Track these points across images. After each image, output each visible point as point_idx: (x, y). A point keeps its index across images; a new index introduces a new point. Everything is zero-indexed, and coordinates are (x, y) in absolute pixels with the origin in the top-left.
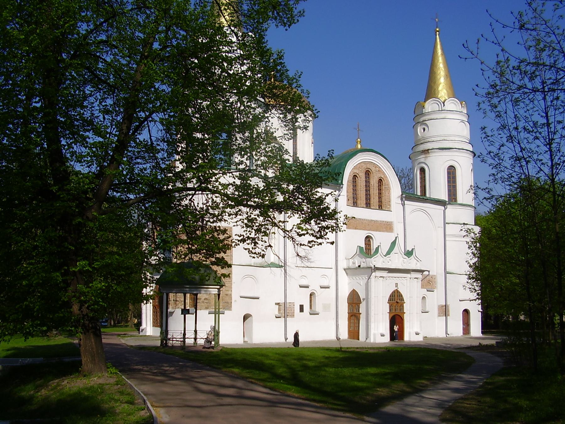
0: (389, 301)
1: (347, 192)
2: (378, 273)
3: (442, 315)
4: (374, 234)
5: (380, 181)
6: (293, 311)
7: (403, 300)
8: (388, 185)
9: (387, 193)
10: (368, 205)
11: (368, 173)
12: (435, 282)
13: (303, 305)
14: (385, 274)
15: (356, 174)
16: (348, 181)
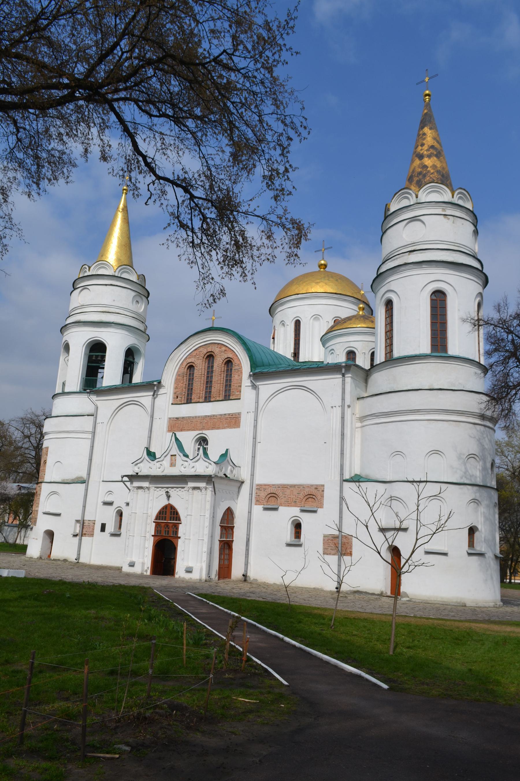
0: (156, 519)
1: (176, 388)
2: (136, 484)
3: (333, 552)
4: (210, 434)
5: (229, 362)
6: (91, 530)
7: (180, 520)
8: (240, 364)
9: (236, 376)
10: (208, 399)
11: (210, 357)
12: (322, 496)
13: (105, 524)
14: (146, 484)
15: (189, 365)
16: (178, 375)
